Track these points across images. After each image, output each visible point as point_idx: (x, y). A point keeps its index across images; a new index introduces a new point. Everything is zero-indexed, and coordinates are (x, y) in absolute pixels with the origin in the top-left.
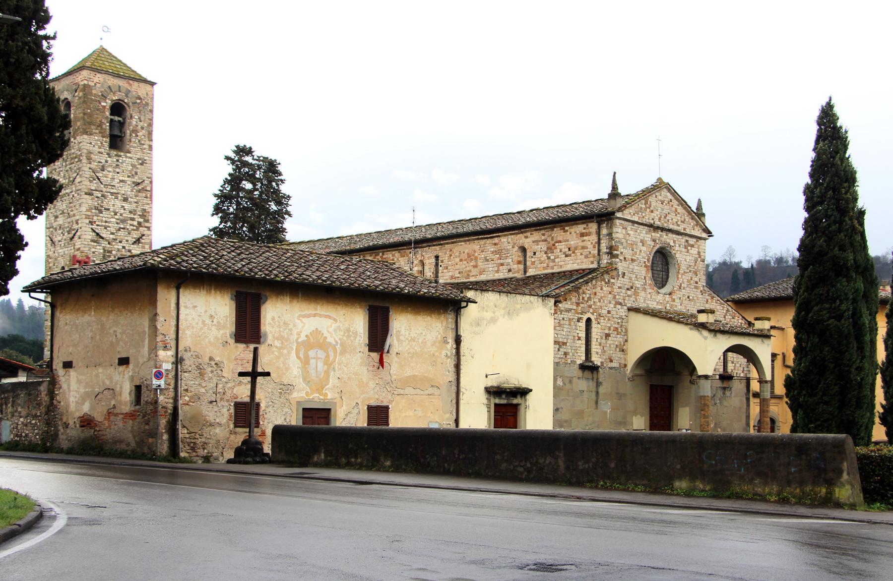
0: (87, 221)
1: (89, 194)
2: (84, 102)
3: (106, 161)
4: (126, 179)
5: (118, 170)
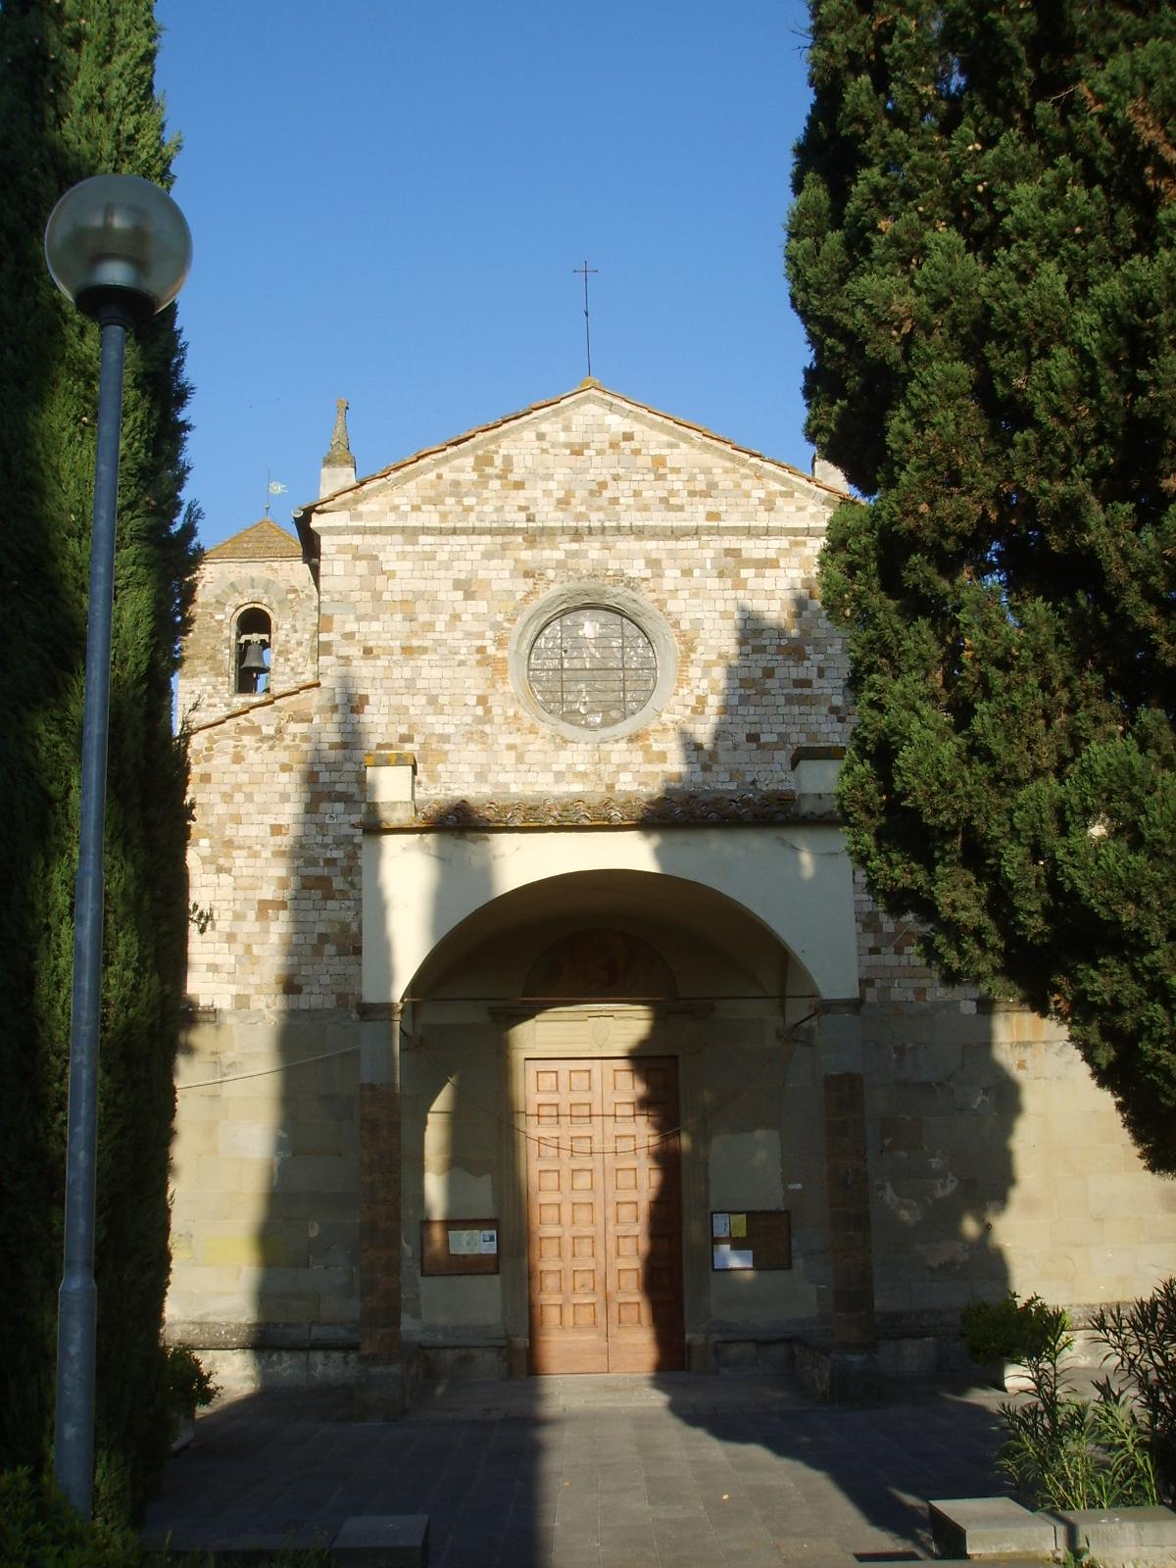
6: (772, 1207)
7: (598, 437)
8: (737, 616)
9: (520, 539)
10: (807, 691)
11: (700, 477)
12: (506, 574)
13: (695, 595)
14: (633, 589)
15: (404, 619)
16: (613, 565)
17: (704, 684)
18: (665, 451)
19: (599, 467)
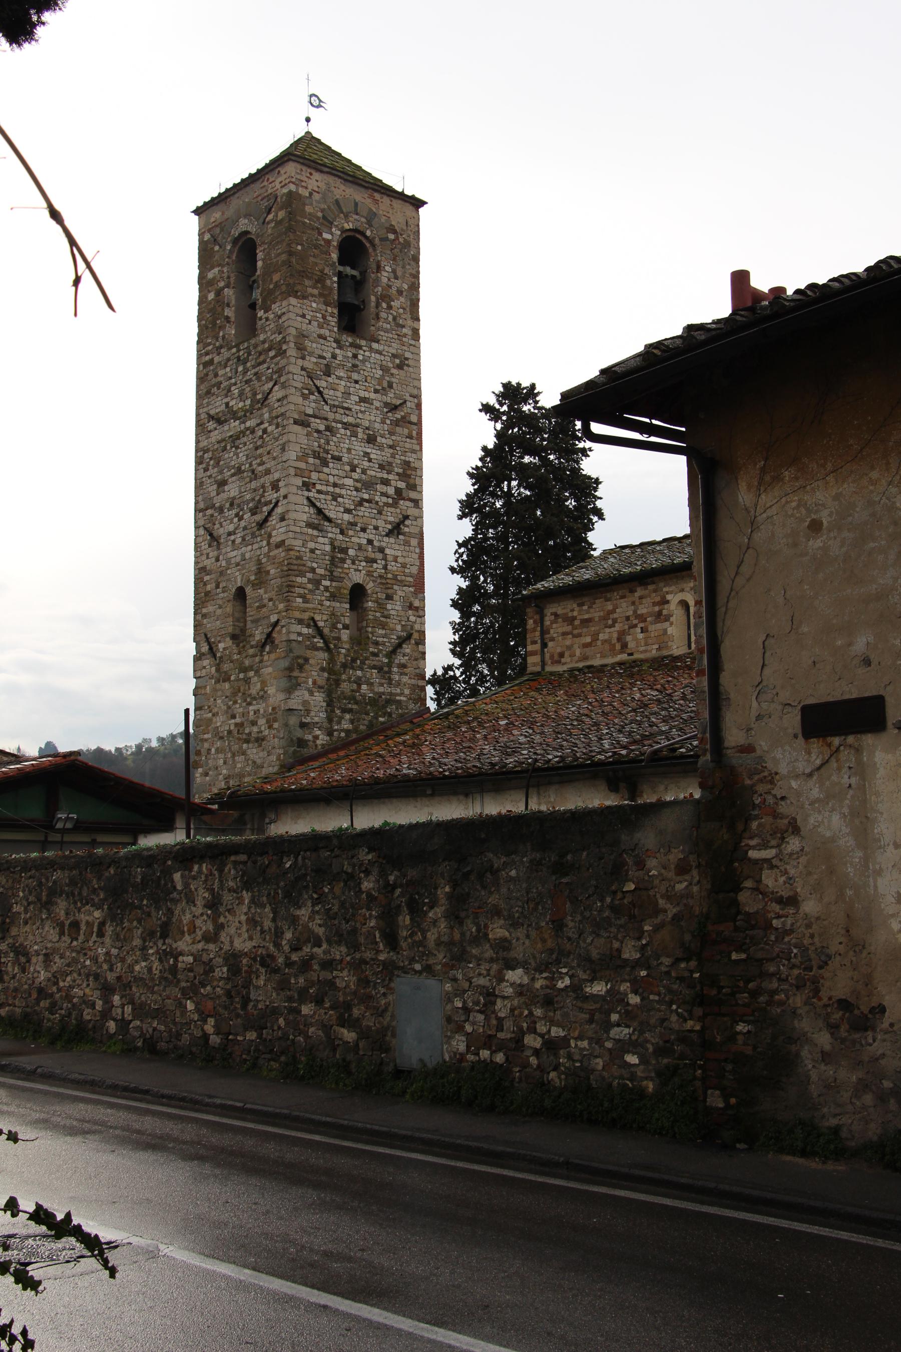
0: (299, 481)
1: (302, 423)
2: (290, 229)
3: (334, 356)
4: (373, 396)
5: (355, 376)
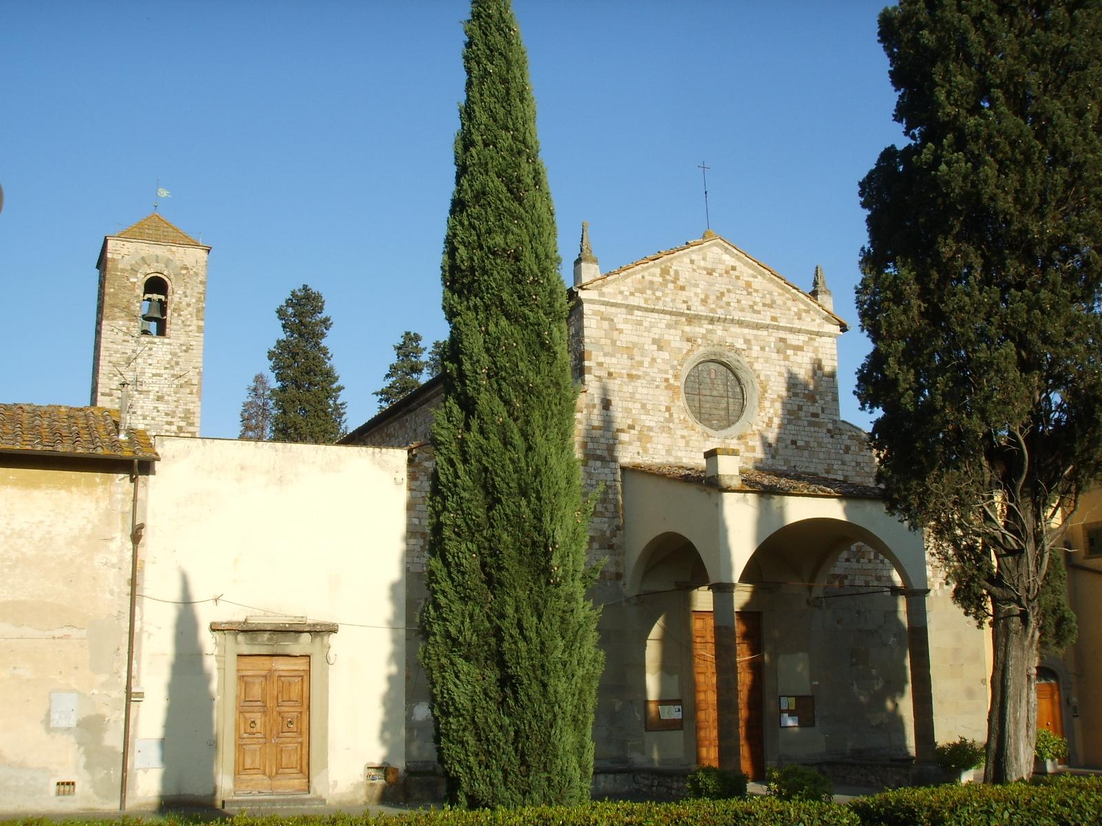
4: (163, 371)
6: (806, 694)
7: (720, 266)
8: (786, 375)
9: (684, 319)
10: (817, 420)
11: (768, 296)
12: (678, 338)
13: (766, 361)
14: (739, 355)
15: (628, 358)
16: (729, 340)
17: (772, 411)
18: (751, 279)
19: (721, 284)
